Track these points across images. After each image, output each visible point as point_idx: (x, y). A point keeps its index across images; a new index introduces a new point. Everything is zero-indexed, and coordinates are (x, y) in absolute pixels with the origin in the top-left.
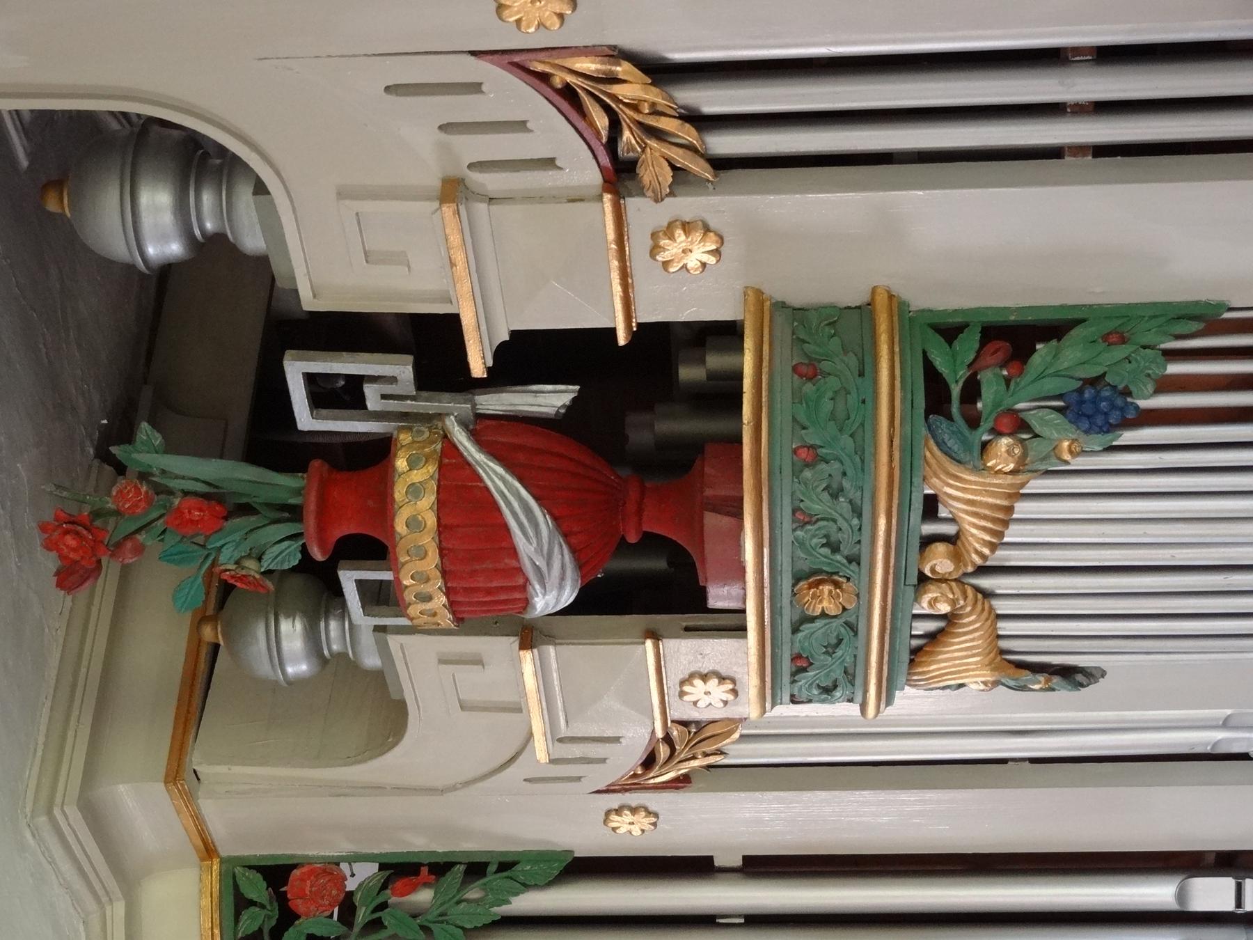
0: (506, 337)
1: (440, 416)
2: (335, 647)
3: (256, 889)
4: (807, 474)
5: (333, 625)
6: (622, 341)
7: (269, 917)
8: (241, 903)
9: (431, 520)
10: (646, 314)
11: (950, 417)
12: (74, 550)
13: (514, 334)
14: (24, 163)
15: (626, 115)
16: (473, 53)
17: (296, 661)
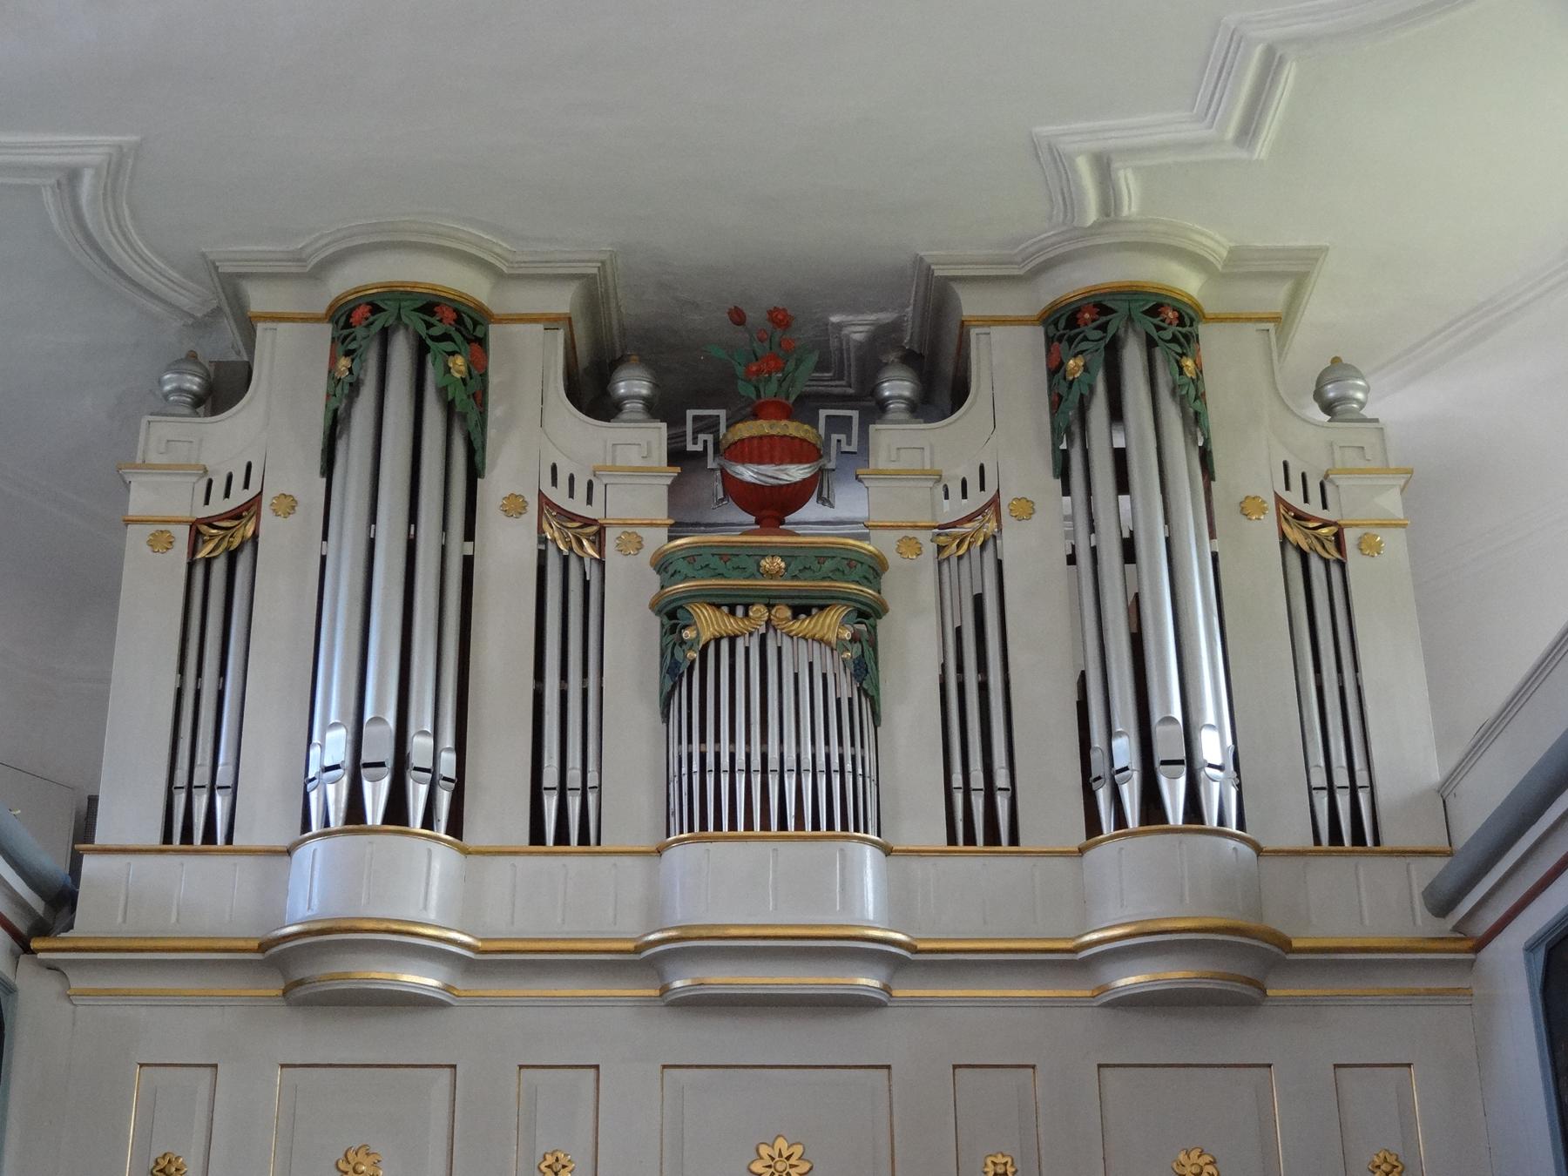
3: (479, 333)
4: (846, 562)
12: (777, 315)
16: (998, 490)
17: (626, 386)
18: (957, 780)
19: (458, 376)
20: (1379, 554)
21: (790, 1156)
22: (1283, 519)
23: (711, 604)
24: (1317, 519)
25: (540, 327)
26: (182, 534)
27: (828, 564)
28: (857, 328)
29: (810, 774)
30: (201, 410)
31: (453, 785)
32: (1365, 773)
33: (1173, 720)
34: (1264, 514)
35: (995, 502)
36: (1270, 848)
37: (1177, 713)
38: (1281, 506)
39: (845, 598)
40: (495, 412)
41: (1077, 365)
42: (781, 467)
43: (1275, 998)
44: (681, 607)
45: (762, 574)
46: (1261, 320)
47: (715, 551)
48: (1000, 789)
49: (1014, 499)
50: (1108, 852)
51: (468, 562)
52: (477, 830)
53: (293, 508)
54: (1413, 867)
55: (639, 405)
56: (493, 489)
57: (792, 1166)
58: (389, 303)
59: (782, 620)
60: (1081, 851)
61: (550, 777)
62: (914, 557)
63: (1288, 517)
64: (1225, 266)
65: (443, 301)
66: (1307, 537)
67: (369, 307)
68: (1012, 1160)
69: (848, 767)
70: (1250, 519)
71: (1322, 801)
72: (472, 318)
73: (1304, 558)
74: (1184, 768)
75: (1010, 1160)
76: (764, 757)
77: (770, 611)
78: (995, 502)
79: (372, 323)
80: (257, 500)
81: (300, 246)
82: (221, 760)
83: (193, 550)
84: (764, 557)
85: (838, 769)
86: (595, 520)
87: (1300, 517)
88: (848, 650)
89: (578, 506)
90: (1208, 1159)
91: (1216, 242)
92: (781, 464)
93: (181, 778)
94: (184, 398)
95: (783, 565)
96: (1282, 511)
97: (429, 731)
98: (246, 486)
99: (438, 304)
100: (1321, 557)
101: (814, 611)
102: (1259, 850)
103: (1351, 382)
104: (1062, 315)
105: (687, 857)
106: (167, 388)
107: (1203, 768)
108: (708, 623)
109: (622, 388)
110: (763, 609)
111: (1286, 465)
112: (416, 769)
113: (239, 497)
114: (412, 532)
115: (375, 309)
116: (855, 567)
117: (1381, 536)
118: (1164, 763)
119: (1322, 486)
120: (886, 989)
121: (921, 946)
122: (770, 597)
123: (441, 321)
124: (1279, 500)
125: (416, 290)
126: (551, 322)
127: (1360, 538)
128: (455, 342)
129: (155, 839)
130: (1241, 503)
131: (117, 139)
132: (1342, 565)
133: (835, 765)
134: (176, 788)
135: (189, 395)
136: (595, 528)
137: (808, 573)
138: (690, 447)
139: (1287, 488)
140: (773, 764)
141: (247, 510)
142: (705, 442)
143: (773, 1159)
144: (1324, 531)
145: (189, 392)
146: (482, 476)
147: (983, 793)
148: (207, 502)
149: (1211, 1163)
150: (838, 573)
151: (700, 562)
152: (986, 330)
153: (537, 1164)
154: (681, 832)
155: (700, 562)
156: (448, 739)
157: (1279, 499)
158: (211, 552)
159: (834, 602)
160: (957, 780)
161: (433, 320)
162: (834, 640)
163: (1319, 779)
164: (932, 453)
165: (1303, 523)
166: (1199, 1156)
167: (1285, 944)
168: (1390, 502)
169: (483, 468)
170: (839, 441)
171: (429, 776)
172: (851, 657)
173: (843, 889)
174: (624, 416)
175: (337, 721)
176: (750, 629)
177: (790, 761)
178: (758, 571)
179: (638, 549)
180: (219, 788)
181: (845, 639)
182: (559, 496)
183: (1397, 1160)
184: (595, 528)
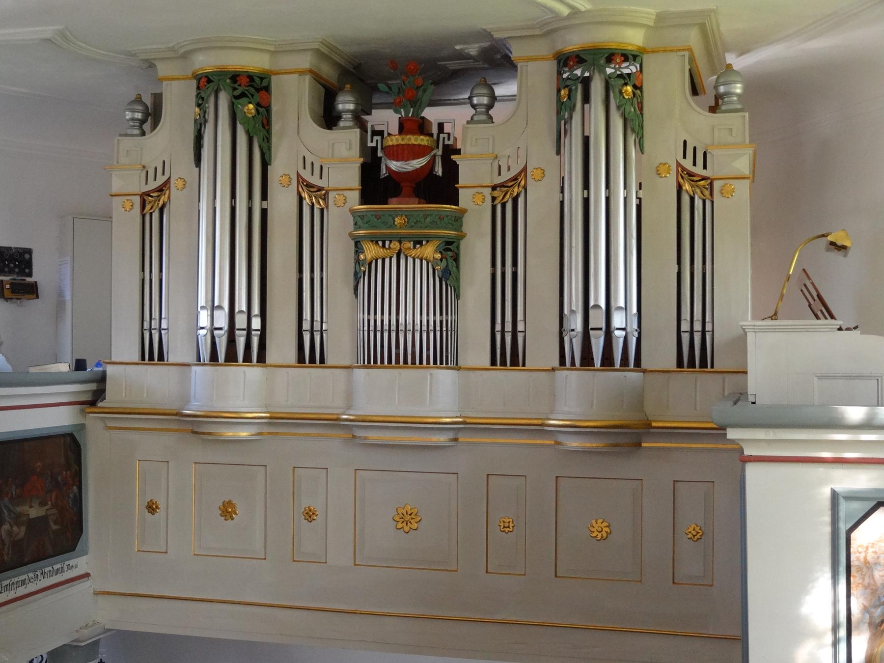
0: (458, 163)
1: (438, 147)
2: (344, 116)
3: (265, 83)
4: (437, 217)
5: (350, 116)
6: (456, 185)
7: (258, 85)
8: (262, 79)
9: (410, 143)
10: (461, 191)
11: (445, 245)
13: (458, 165)
14: (439, 63)
15: (511, 188)
18: (498, 327)
19: (250, 116)
20: (732, 196)
21: (412, 513)
22: (680, 176)
23: (372, 241)
24: (699, 176)
25: (296, 76)
26: (137, 200)
27: (428, 220)
28: (473, 50)
29: (419, 332)
30: (147, 127)
31: (259, 332)
32: (710, 325)
33: (597, 306)
34: (669, 173)
35: (525, 169)
36: (650, 369)
37: (602, 303)
38: (679, 169)
39: (437, 237)
40: (275, 127)
41: (565, 94)
42: (406, 163)
43: (646, 447)
44: (359, 241)
45: (396, 226)
46: (680, 50)
47: (374, 213)
48: (519, 332)
49: (534, 169)
50: (562, 374)
51: (264, 213)
52: (272, 356)
53: (184, 185)
54: (726, 379)
55: (349, 116)
56: (276, 171)
57: (412, 519)
58: (214, 77)
59: (406, 249)
60: (553, 369)
61: (306, 326)
62: (481, 203)
63: (683, 175)
64: (655, 22)
65: (243, 74)
66: (692, 186)
67: (206, 79)
68: (513, 520)
69: (438, 328)
70: (661, 177)
71: (685, 338)
72: (258, 77)
73: (692, 200)
74: (601, 335)
75: (511, 520)
76: (398, 321)
77: (400, 245)
78: (525, 169)
79: (207, 88)
80: (168, 181)
81: (172, 45)
82: (163, 316)
83: (143, 207)
84: (397, 216)
85: (433, 329)
86: (323, 187)
87: (690, 174)
88: (438, 265)
89: (315, 180)
90: (605, 524)
91: (648, 13)
92: (408, 160)
93: (146, 326)
94: (136, 124)
95: (407, 220)
96: (680, 171)
97: (245, 311)
98: (163, 174)
99: (238, 76)
100: (700, 198)
101: (424, 243)
102: (644, 371)
103: (733, 85)
104: (562, 59)
105: (361, 374)
106: (127, 117)
107: (614, 331)
108: (371, 251)
109: (340, 107)
110: (398, 244)
111: (685, 142)
112: (238, 329)
113: (161, 180)
114: (233, 204)
115: (209, 81)
116: (443, 218)
117: (735, 184)
118: (592, 329)
119: (705, 154)
120: (456, 440)
121: (468, 420)
122: (400, 238)
123: (240, 85)
124: (678, 164)
125: (226, 70)
126: (302, 73)
127: (722, 186)
128: (248, 97)
129: (136, 357)
130: (657, 167)
131: (56, 27)
132: (712, 202)
133: (431, 328)
134: (145, 330)
135: (137, 122)
136: (324, 192)
137: (419, 225)
138: (370, 144)
139: (685, 157)
140: (402, 327)
141: (165, 186)
142: (377, 140)
143: (403, 515)
144: (702, 183)
145: (137, 119)
146: (270, 165)
147: (510, 333)
148: (147, 183)
149: (607, 527)
150: (434, 225)
151: (366, 220)
152: (526, 64)
153: (302, 512)
154: (358, 364)
155: (366, 220)
156: (256, 310)
157: (678, 164)
158: (151, 208)
159: (431, 239)
160: (498, 327)
161: (236, 86)
162: (431, 259)
163: (685, 326)
164: (494, 141)
165: (691, 178)
166: (602, 523)
167: (648, 425)
168: (743, 165)
169: (270, 160)
170: (444, 138)
171: (245, 332)
172: (440, 269)
173: (431, 393)
174: (342, 124)
175: (204, 305)
176: (390, 255)
177: (410, 327)
178: (394, 223)
179: (344, 203)
180: (163, 329)
181: (437, 259)
182: (306, 175)
183: (700, 529)
184: (324, 192)
